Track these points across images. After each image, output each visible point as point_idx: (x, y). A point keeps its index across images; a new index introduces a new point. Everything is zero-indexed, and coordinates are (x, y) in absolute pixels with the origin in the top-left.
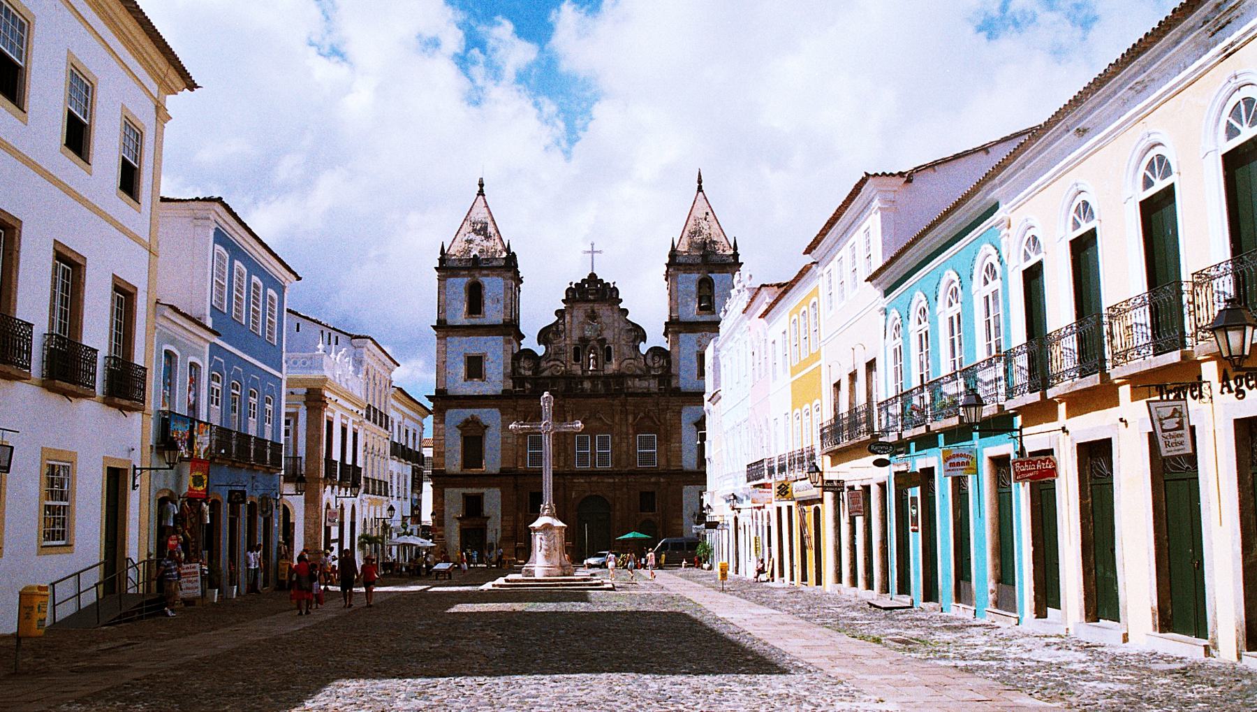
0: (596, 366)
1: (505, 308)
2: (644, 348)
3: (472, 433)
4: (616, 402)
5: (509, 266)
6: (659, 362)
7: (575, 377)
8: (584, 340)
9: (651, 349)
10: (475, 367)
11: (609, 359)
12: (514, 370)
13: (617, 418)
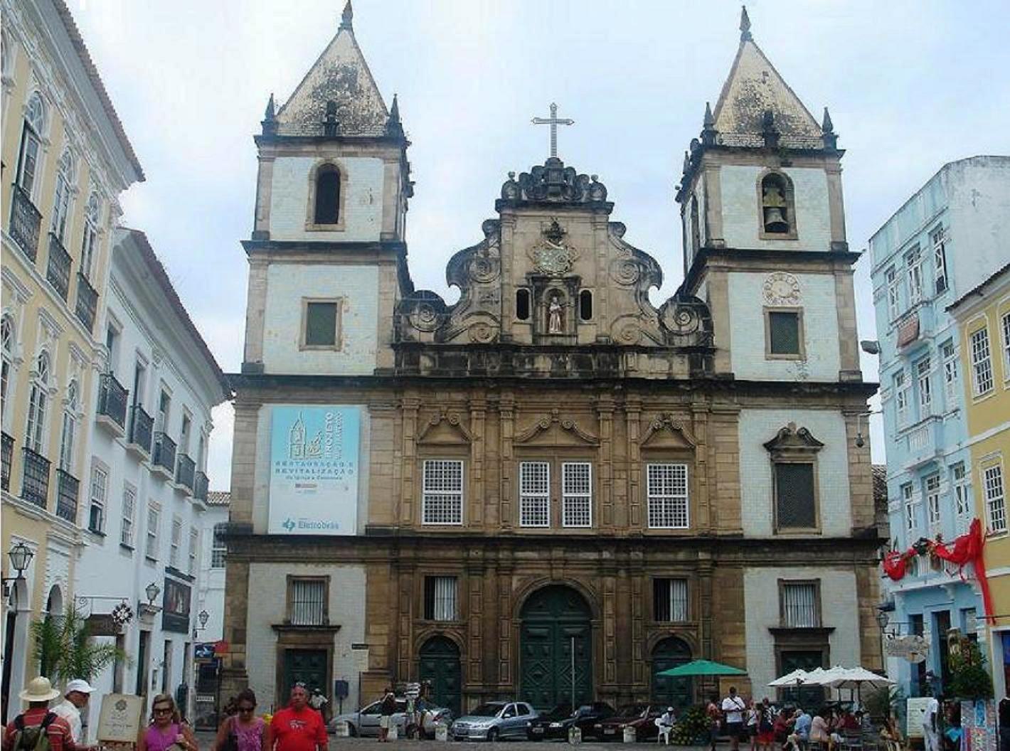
0: (562, 326)
1: (385, 211)
2: (658, 297)
4: (605, 397)
5: (392, 138)
7: (517, 348)
8: (538, 280)
10: (321, 322)
11: (587, 314)
12: (398, 334)
13: (606, 429)
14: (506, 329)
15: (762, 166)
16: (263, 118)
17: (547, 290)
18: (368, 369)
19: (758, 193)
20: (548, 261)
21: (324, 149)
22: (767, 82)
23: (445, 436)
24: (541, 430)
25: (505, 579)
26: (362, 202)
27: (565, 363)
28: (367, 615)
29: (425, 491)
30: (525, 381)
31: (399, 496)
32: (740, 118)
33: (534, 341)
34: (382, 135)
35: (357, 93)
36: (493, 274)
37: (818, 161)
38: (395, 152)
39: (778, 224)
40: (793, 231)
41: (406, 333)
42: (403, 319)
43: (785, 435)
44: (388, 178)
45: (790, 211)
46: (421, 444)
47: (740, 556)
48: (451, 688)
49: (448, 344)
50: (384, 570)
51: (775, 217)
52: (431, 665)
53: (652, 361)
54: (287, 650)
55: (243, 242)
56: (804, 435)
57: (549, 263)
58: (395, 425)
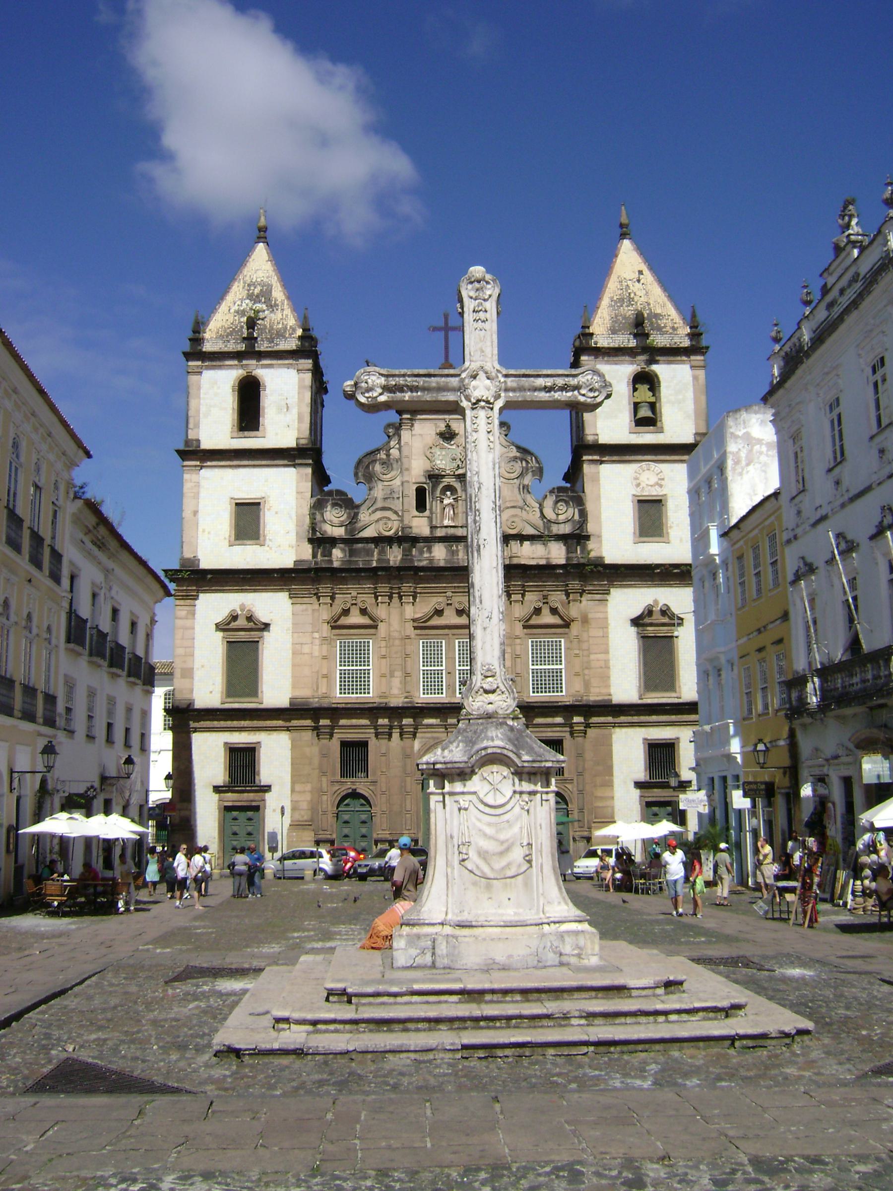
3: (242, 636)
6: (568, 512)
8: (434, 477)
9: (552, 492)
10: (248, 519)
12: (313, 528)
14: (406, 522)
15: (632, 364)
16: (190, 335)
17: (441, 486)
18: (289, 563)
19: (629, 390)
20: (441, 460)
21: (245, 362)
22: (642, 282)
23: (355, 618)
24: (439, 613)
25: (407, 742)
26: (279, 410)
27: (458, 551)
28: (293, 776)
29: (339, 668)
30: (423, 569)
31: (318, 672)
32: (615, 320)
33: (431, 532)
34: (295, 348)
35: (272, 306)
36: (393, 474)
37: (684, 358)
38: (308, 363)
39: (647, 420)
40: (659, 424)
41: (321, 528)
42: (318, 517)
43: (649, 612)
44: (301, 387)
45: (658, 405)
46: (335, 625)
47: (610, 719)
48: (364, 836)
49: (357, 537)
50: (308, 735)
51: (645, 412)
52: (346, 817)
53: (534, 546)
54: (225, 807)
55: (178, 451)
56: (665, 612)
57: (443, 462)
58: (313, 610)
